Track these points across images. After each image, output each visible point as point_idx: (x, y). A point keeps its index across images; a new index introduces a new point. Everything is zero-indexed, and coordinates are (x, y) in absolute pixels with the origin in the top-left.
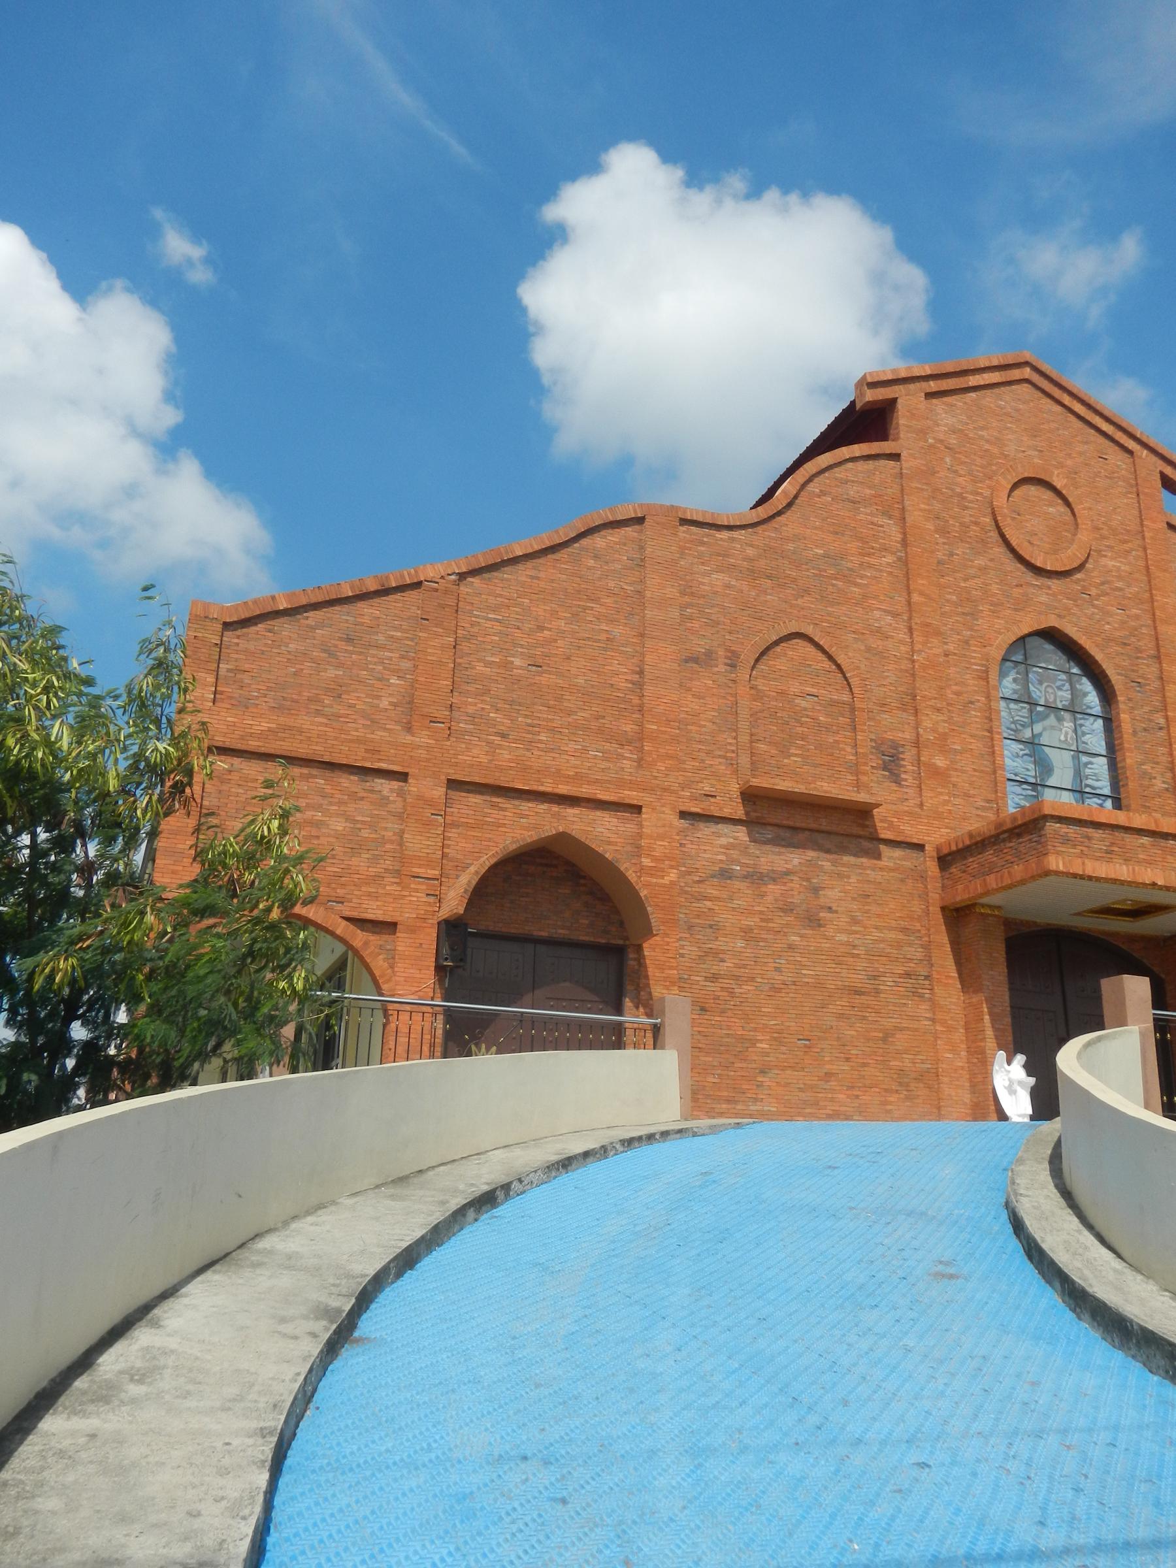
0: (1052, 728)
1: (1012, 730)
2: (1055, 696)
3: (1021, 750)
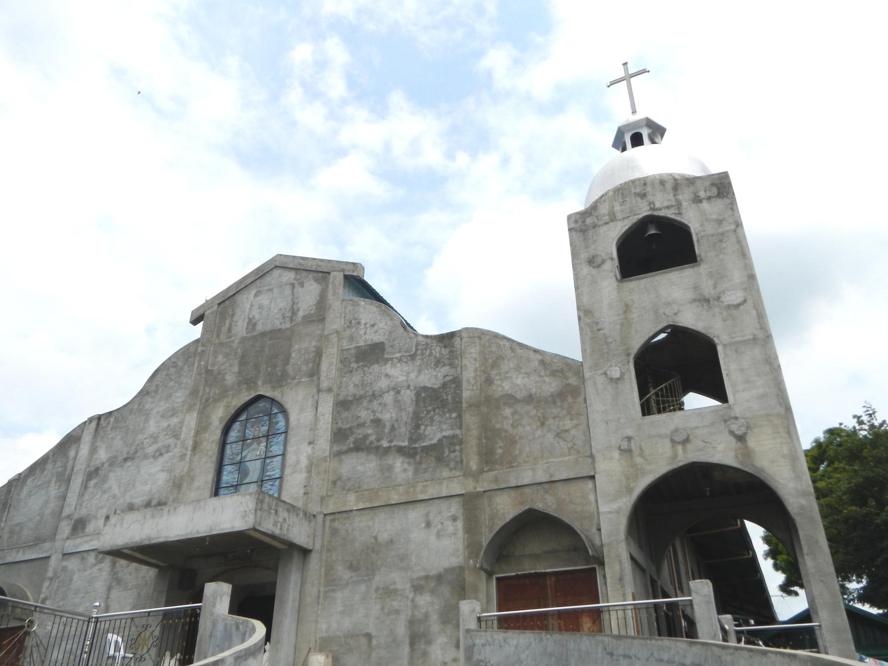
0: (254, 450)
2: (260, 430)
3: (233, 468)
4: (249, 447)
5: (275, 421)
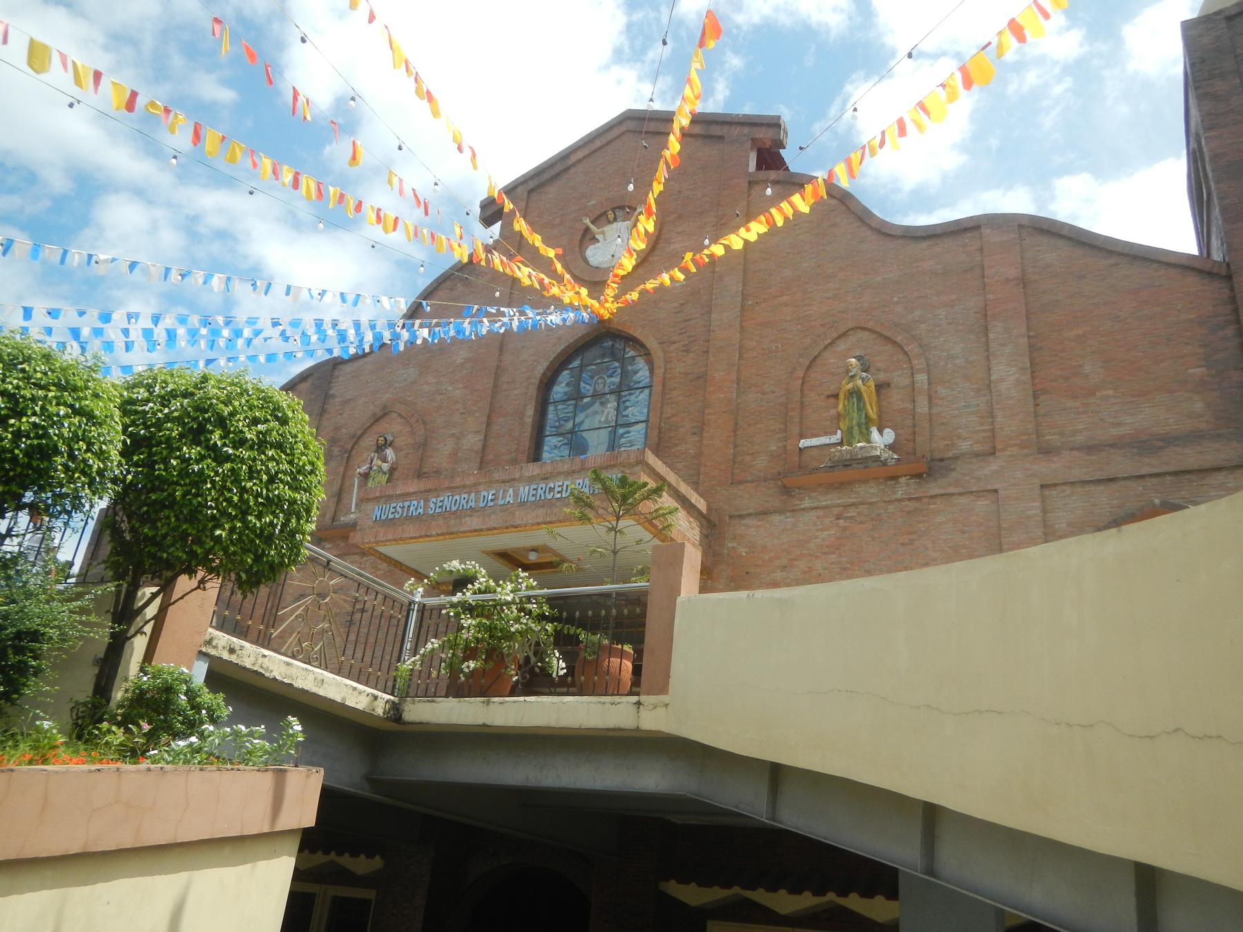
0: (596, 413)
1: (555, 427)
4: (585, 410)
5: (632, 370)
